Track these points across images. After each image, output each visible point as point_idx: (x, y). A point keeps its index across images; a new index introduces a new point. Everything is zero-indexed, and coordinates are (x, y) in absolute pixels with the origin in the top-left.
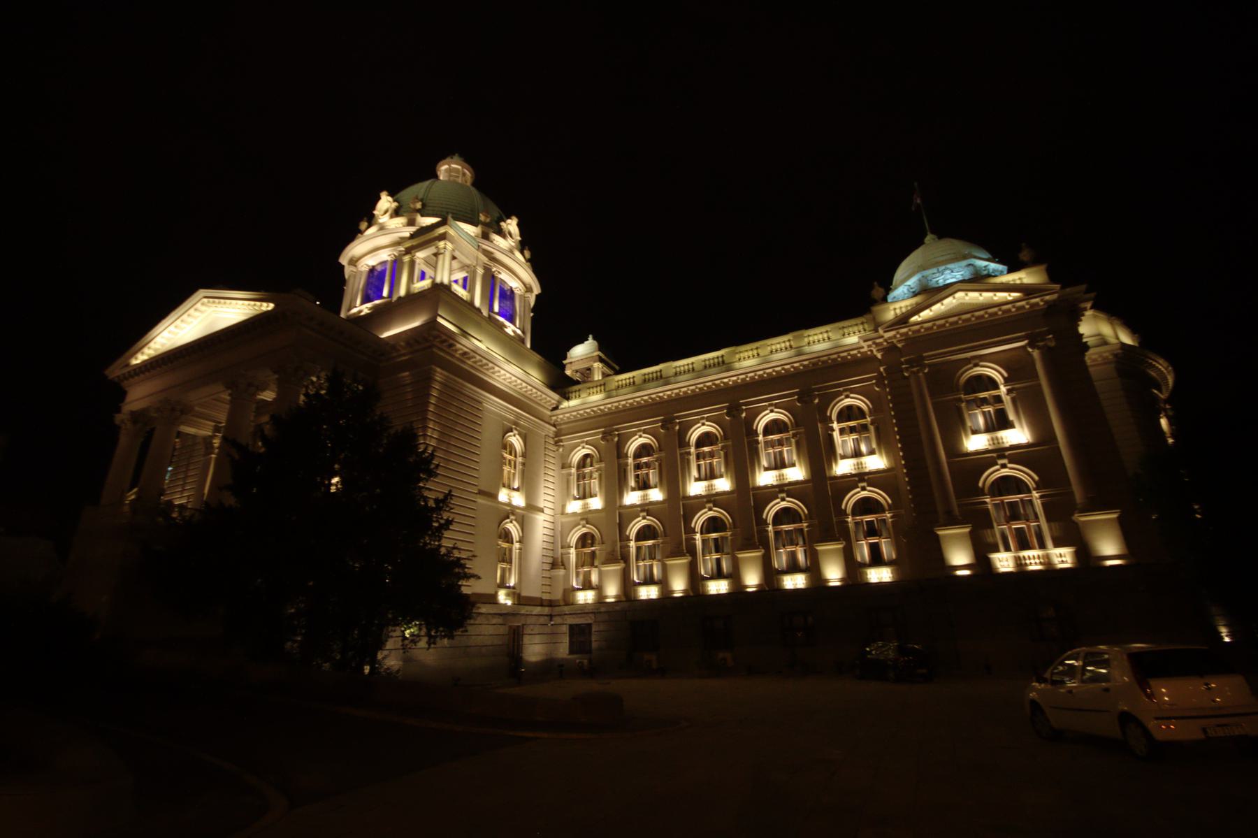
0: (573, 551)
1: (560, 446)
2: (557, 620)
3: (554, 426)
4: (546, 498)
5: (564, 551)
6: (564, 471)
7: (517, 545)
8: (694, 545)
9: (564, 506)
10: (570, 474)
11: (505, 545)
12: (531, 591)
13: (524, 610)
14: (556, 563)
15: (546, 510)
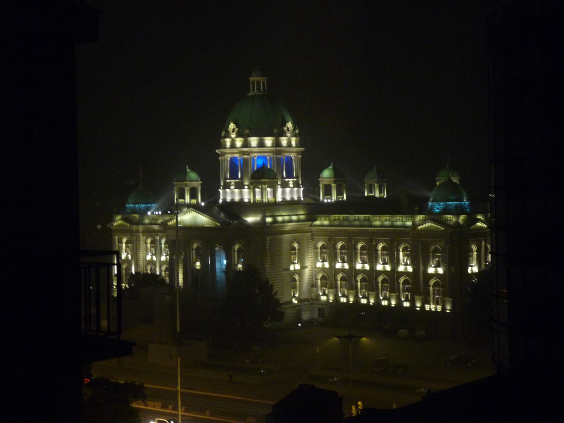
0: (319, 281)
1: (313, 241)
2: (314, 306)
3: (311, 232)
4: (308, 263)
5: (316, 281)
6: (315, 250)
7: (298, 282)
8: (357, 286)
9: (315, 264)
10: (317, 252)
11: (294, 283)
12: (304, 297)
13: (303, 303)
14: (313, 285)
15: (309, 267)
